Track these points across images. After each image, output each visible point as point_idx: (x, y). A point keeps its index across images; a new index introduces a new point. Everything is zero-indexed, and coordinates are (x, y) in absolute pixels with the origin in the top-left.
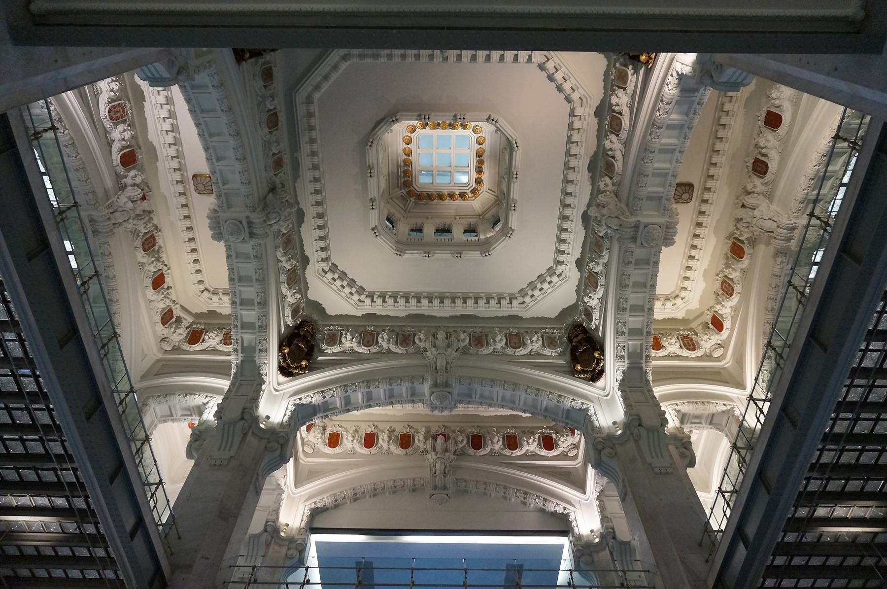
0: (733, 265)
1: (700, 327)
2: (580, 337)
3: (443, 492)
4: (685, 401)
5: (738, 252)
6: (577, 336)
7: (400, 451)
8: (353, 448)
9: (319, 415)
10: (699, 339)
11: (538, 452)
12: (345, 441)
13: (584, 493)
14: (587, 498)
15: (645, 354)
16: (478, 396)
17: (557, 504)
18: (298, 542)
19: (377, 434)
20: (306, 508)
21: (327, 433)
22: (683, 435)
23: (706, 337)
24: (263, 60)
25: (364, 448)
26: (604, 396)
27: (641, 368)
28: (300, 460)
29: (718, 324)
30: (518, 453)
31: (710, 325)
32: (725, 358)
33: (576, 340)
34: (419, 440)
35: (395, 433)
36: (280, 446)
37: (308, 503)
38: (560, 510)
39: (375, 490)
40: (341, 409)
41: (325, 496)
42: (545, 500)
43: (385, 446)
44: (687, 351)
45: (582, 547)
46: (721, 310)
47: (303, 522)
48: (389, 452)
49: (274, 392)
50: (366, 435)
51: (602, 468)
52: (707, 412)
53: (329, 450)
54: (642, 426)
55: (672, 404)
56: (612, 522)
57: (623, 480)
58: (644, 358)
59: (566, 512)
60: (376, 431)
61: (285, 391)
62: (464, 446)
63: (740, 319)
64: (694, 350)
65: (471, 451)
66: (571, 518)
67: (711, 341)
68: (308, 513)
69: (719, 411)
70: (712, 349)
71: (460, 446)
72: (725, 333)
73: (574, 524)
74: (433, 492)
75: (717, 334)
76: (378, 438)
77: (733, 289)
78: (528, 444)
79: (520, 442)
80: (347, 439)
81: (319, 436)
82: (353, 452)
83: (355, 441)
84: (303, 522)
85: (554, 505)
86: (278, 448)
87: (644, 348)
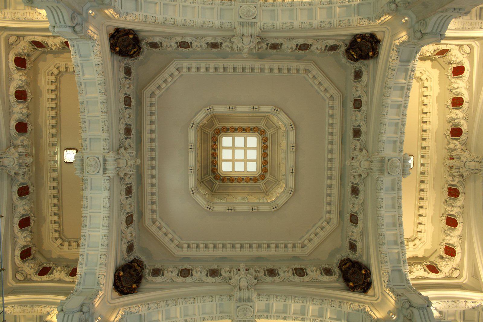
2: (353, 53)
6: (352, 55)
7: (461, 198)
8: (457, 236)
11: (466, 79)
12: (451, 242)
19: (447, 215)
21: (445, 256)
24: (147, 274)
25: (457, 227)
26: (389, 31)
28: (464, 282)
30: (466, 98)
35: (448, 200)
36: (410, 308)
40: (400, 250)
48: (462, 207)
49: (379, 300)
50: (447, 224)
53: (458, 257)
57: (442, 12)
60: (445, 215)
65: (463, 137)
71: (459, 146)
76: (451, 215)
81: (444, 263)
82: (461, 237)
83: (451, 234)
86: (411, 310)
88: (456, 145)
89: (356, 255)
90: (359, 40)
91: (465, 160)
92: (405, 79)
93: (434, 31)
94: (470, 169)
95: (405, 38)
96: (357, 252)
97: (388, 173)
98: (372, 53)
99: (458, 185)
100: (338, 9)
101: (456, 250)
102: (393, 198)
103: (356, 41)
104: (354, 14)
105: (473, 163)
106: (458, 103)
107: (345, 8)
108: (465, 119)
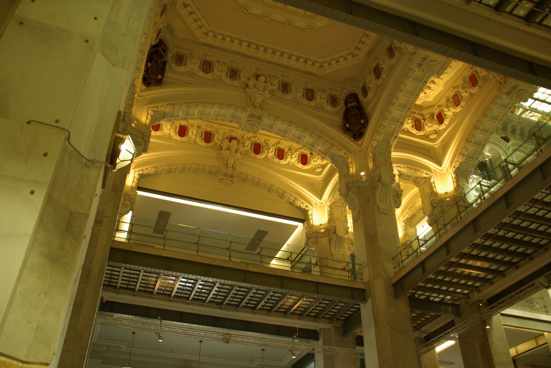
0: (467, 88)
1: (428, 116)
2: (353, 104)
3: (229, 179)
4: (405, 166)
5: (473, 81)
6: (352, 102)
8: (169, 134)
9: (166, 119)
10: (425, 124)
11: (296, 165)
13: (321, 199)
14: (321, 202)
15: (395, 135)
16: (277, 128)
17: (302, 202)
18: (131, 197)
20: (136, 174)
22: (399, 189)
23: (430, 124)
25: (178, 136)
26: (359, 151)
27: (389, 142)
29: (440, 119)
30: (283, 162)
31: (435, 117)
32: (436, 141)
33: (350, 105)
34: (218, 139)
36: (144, 142)
37: (137, 170)
38: (303, 206)
39: (184, 168)
41: (149, 167)
42: (296, 198)
43: (193, 137)
44: (415, 130)
45: (312, 232)
46: (446, 111)
47: (134, 183)
51: (347, 198)
52: (415, 175)
54: (380, 182)
55: (398, 167)
56: (335, 223)
57: (359, 211)
58: (394, 137)
59: (307, 209)
61: (145, 97)
62: (248, 150)
63: (454, 125)
64: (419, 130)
65: (253, 154)
66: (310, 213)
67: (432, 128)
68: (137, 176)
69: (422, 176)
70: (431, 132)
71: (246, 149)
72: (442, 127)
73: (310, 217)
74: (223, 177)
75: (437, 124)
77: (460, 103)
78: (292, 158)
79: (286, 155)
80: (166, 126)
82: (169, 138)
84: (134, 183)
85: (301, 202)
87: (396, 131)
88: (247, 146)
89: (173, 64)
90: (362, 121)
91: (236, 156)
92: (319, 150)
93: (348, 196)
94: (228, 159)
95: (351, 170)
96: (174, 65)
97: (248, 121)
98: (348, 126)
99: (214, 142)
100: (394, 127)
101: (158, 132)
102: (225, 116)
103: (363, 118)
104: (384, 138)
105: (232, 162)
106: (280, 154)
107: (392, 131)
108: (266, 157)
